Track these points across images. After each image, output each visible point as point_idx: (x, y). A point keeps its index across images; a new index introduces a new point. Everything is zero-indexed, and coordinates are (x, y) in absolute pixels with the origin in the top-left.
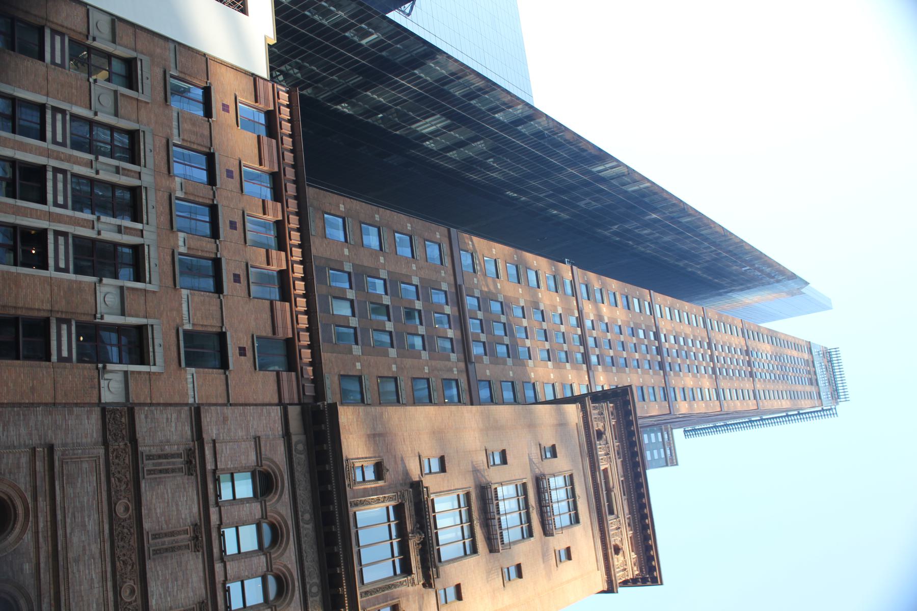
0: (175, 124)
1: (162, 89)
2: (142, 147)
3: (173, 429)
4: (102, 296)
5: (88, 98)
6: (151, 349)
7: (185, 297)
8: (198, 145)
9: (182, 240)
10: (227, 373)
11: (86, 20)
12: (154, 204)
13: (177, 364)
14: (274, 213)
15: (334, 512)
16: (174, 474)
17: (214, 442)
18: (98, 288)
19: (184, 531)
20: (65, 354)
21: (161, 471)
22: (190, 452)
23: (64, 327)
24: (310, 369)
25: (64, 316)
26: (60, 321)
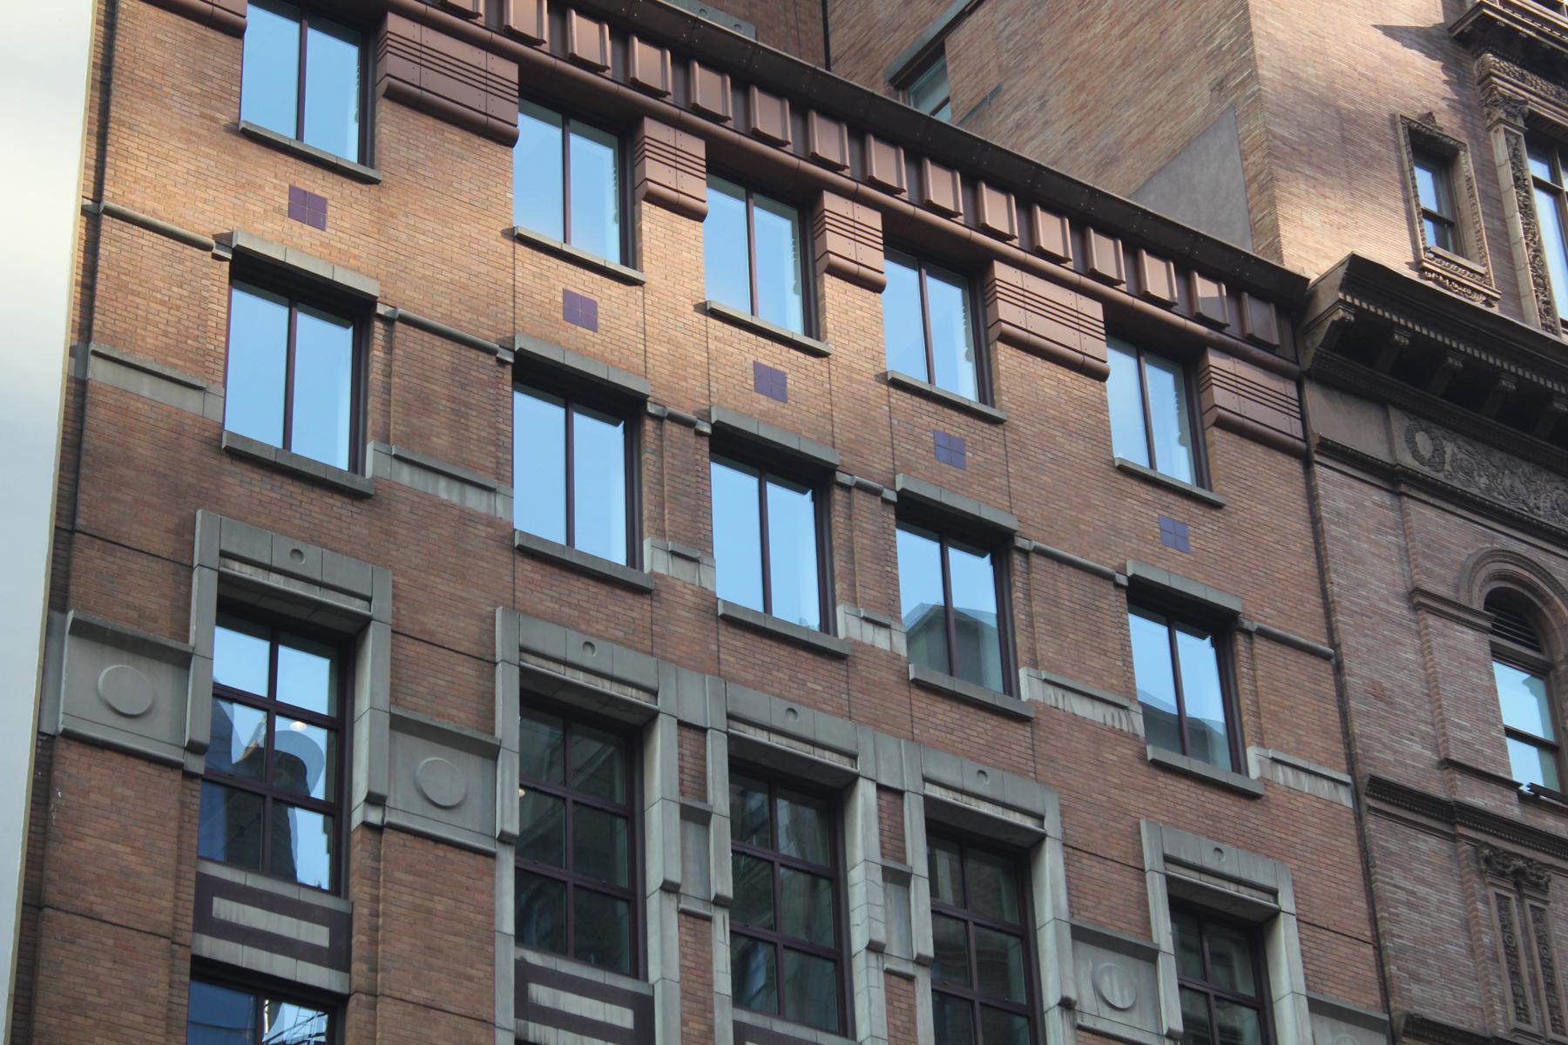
0: (444, 490)
1: (315, 494)
2: (580, 678)
3: (1434, 897)
4: (1106, 1012)
5: (453, 855)
6: (1231, 889)
7: (1051, 696)
8: (389, 365)
9: (868, 628)
10: (1247, 624)
11: (118, 759)
12: (576, 639)
13: (1244, 802)
14: (852, 234)
15: (1469, 360)
16: (1498, 924)
17: (1448, 764)
18: (1088, 1023)
19: (1500, 909)
20: (224, 909)
21: (1551, 986)
22: (1493, 865)
23: (224, 909)
24: (1206, 289)
25: (358, 939)
26: (206, 923)
